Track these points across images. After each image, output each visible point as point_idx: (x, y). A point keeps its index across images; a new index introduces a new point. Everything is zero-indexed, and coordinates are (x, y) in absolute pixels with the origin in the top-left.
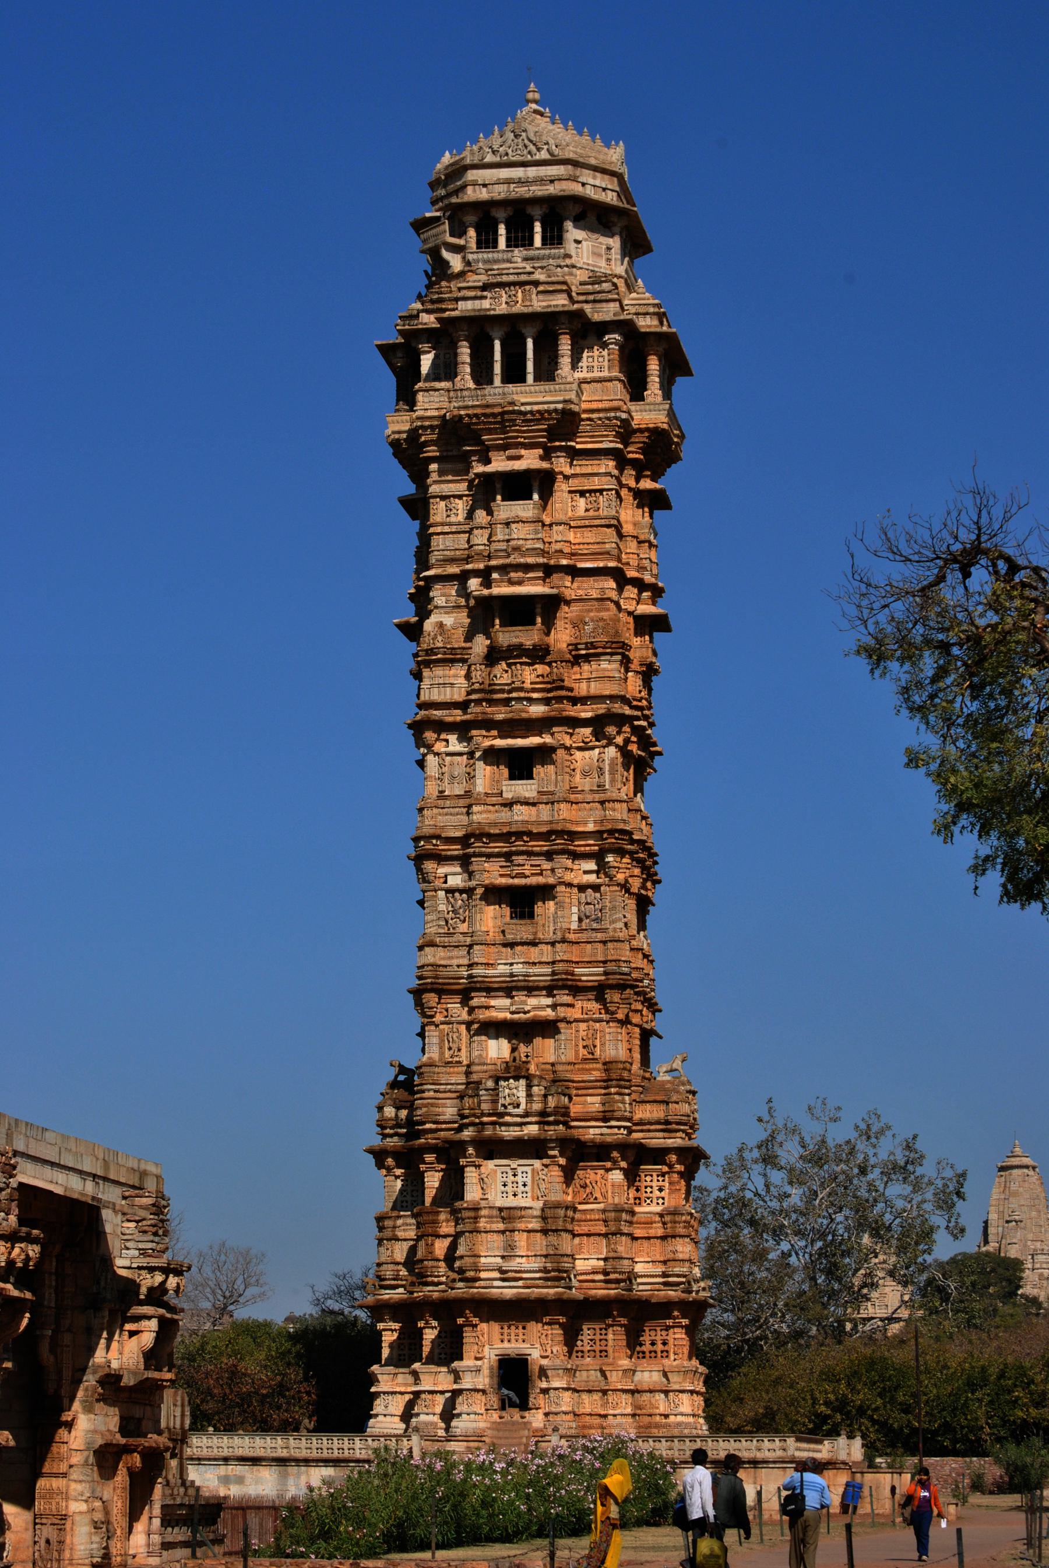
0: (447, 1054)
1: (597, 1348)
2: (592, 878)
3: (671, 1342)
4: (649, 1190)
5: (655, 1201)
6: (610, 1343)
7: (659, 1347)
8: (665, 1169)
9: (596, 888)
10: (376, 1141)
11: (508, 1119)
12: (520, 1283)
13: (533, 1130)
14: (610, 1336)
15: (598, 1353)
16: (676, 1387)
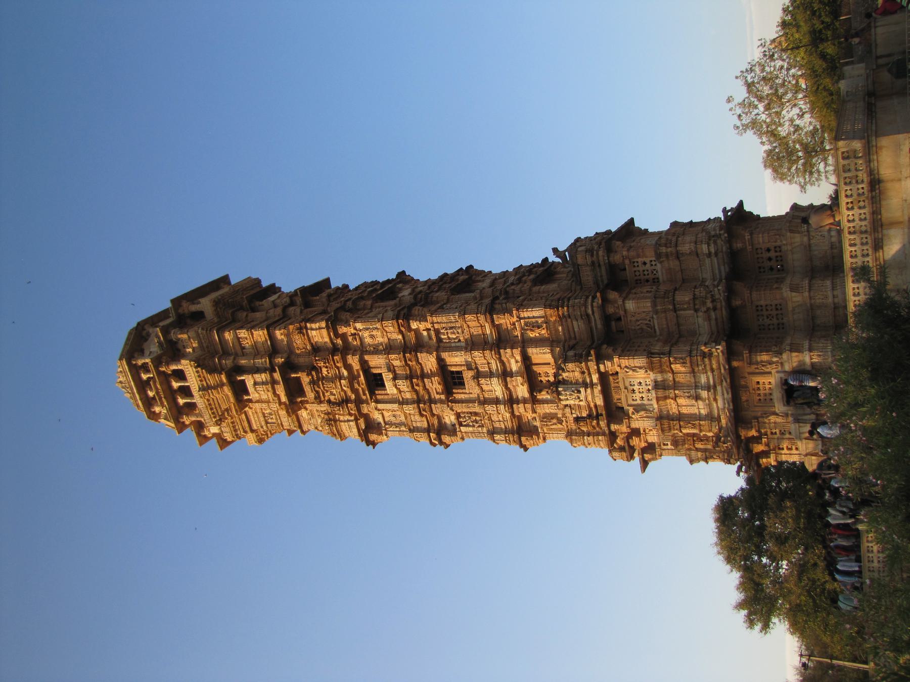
0: (559, 426)
1: (774, 313)
2: (432, 333)
3: (768, 245)
4: (646, 273)
5: (653, 267)
6: (768, 302)
7: (772, 254)
8: (627, 262)
9: (437, 332)
10: (637, 459)
11: (590, 398)
12: (719, 388)
13: (595, 377)
14: (762, 303)
15: (779, 312)
16: (805, 239)
